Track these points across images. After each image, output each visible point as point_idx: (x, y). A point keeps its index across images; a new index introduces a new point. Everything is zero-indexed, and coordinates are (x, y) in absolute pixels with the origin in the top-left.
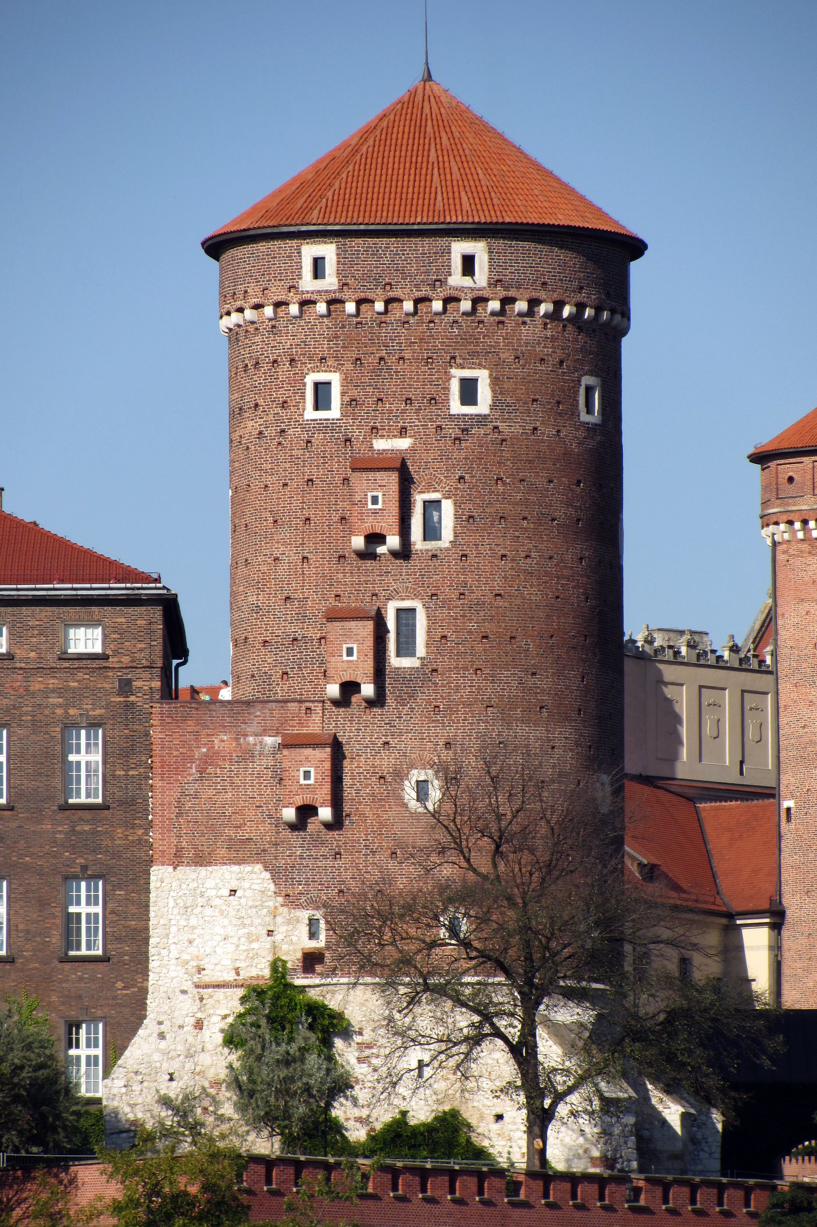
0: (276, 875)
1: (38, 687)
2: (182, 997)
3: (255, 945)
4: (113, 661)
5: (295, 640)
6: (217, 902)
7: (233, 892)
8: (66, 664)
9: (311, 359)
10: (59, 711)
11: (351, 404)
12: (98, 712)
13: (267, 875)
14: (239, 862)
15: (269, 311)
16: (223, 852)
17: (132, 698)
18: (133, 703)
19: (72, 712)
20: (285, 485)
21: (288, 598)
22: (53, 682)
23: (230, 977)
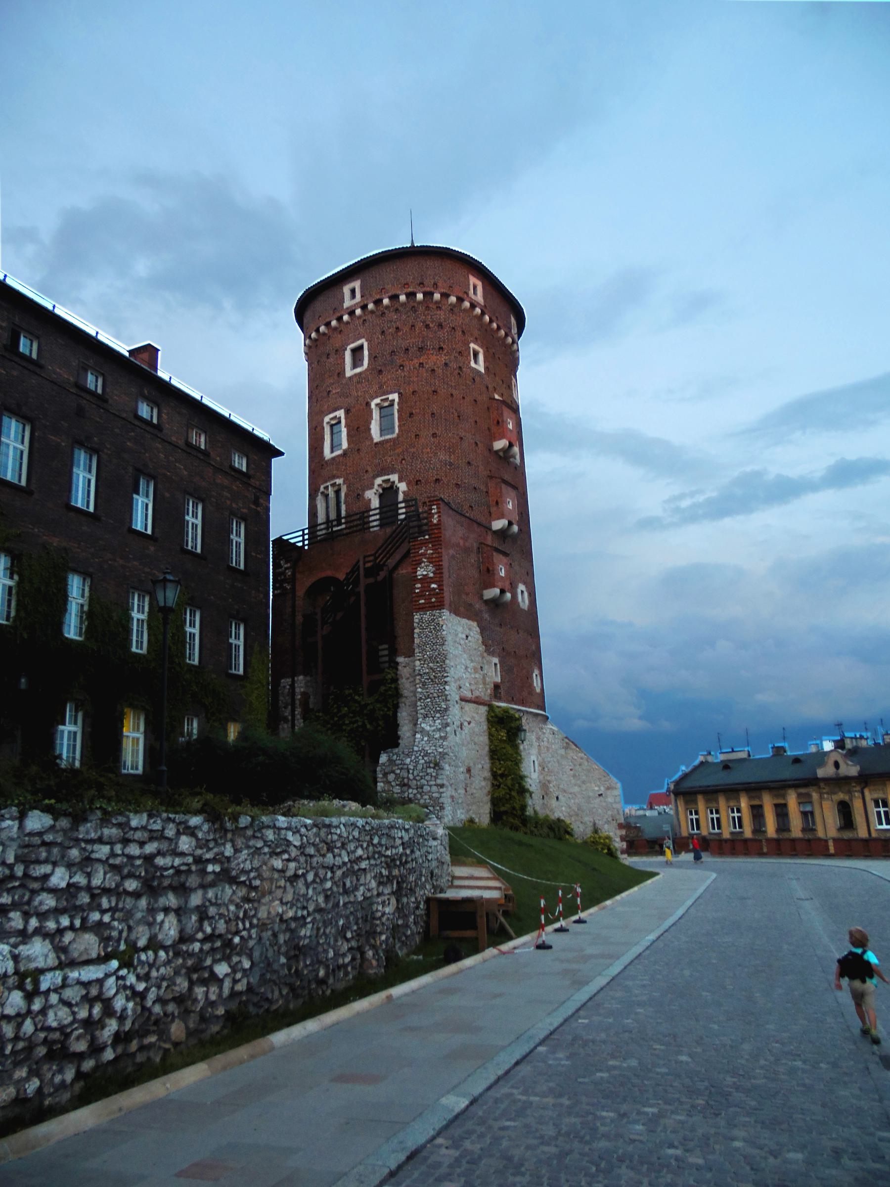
0: (483, 630)
1: (218, 481)
2: (457, 706)
3: (477, 676)
4: (252, 481)
5: (475, 488)
6: (462, 642)
7: (467, 637)
8: (233, 473)
9: (472, 335)
10: (228, 502)
11: (486, 368)
12: (245, 511)
13: (478, 629)
14: (469, 618)
15: (453, 299)
16: (462, 609)
17: (258, 509)
18: (258, 512)
19: (234, 505)
20: (464, 398)
21: (469, 463)
22: (226, 482)
23: (468, 695)
